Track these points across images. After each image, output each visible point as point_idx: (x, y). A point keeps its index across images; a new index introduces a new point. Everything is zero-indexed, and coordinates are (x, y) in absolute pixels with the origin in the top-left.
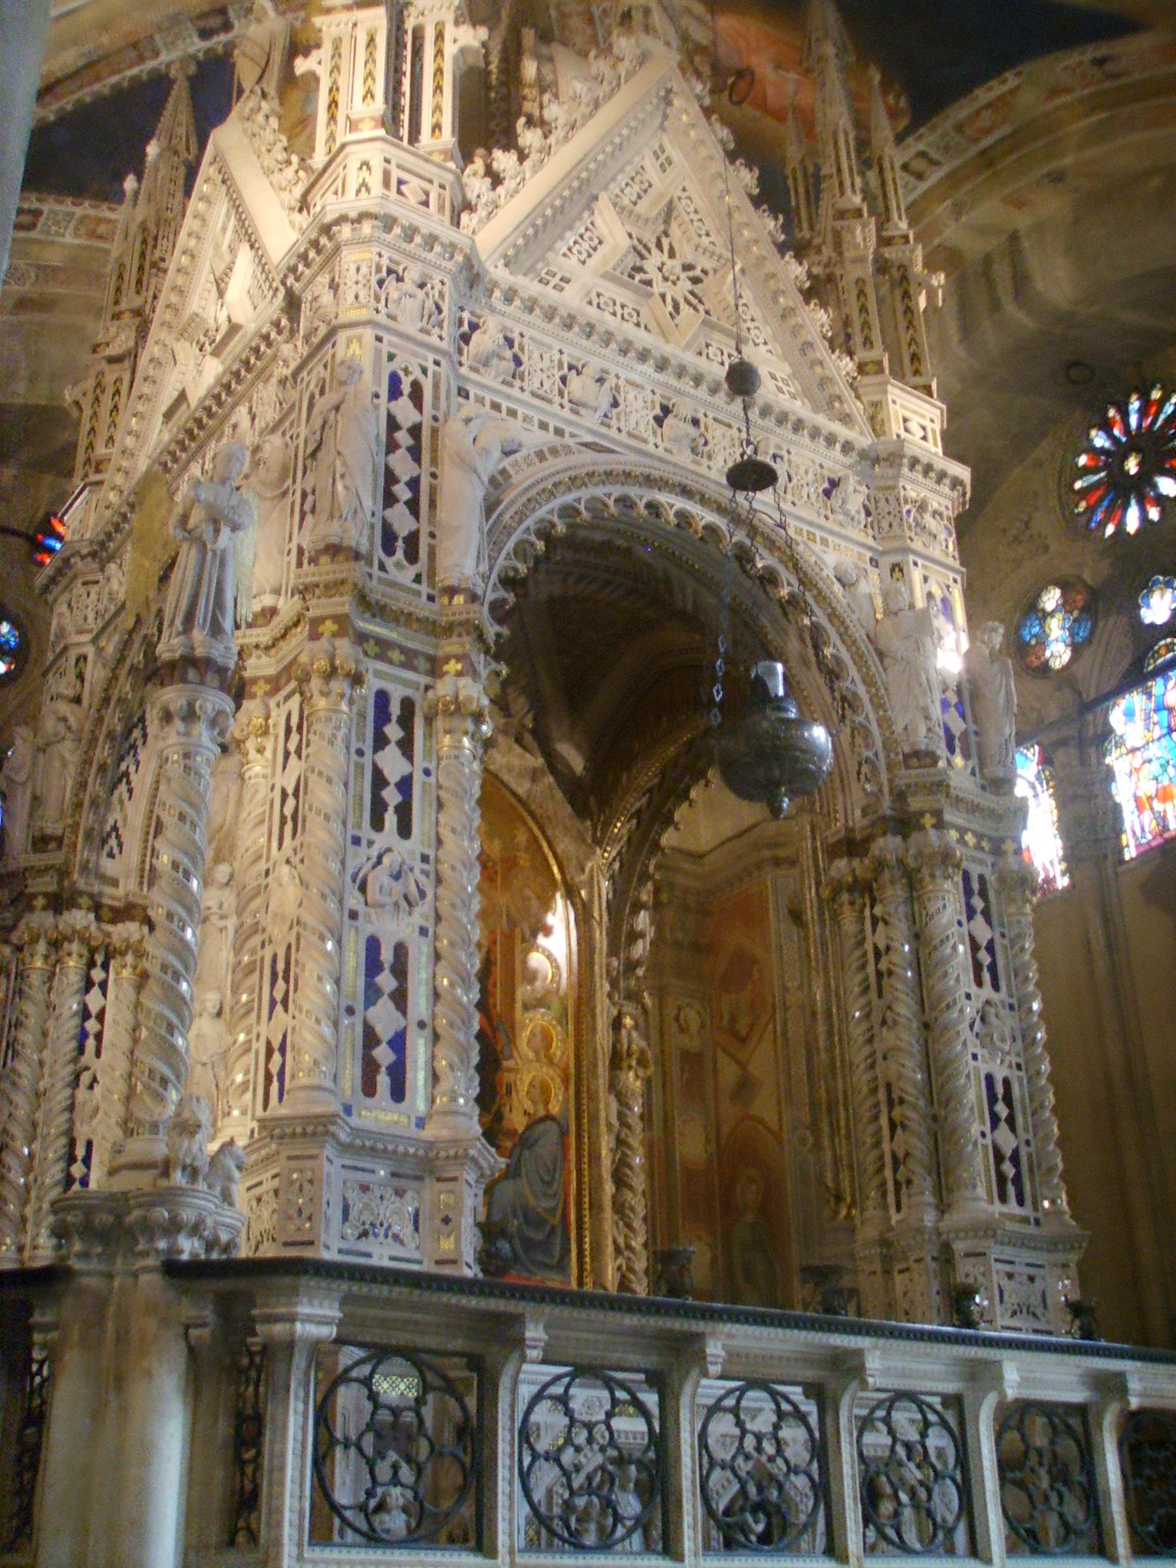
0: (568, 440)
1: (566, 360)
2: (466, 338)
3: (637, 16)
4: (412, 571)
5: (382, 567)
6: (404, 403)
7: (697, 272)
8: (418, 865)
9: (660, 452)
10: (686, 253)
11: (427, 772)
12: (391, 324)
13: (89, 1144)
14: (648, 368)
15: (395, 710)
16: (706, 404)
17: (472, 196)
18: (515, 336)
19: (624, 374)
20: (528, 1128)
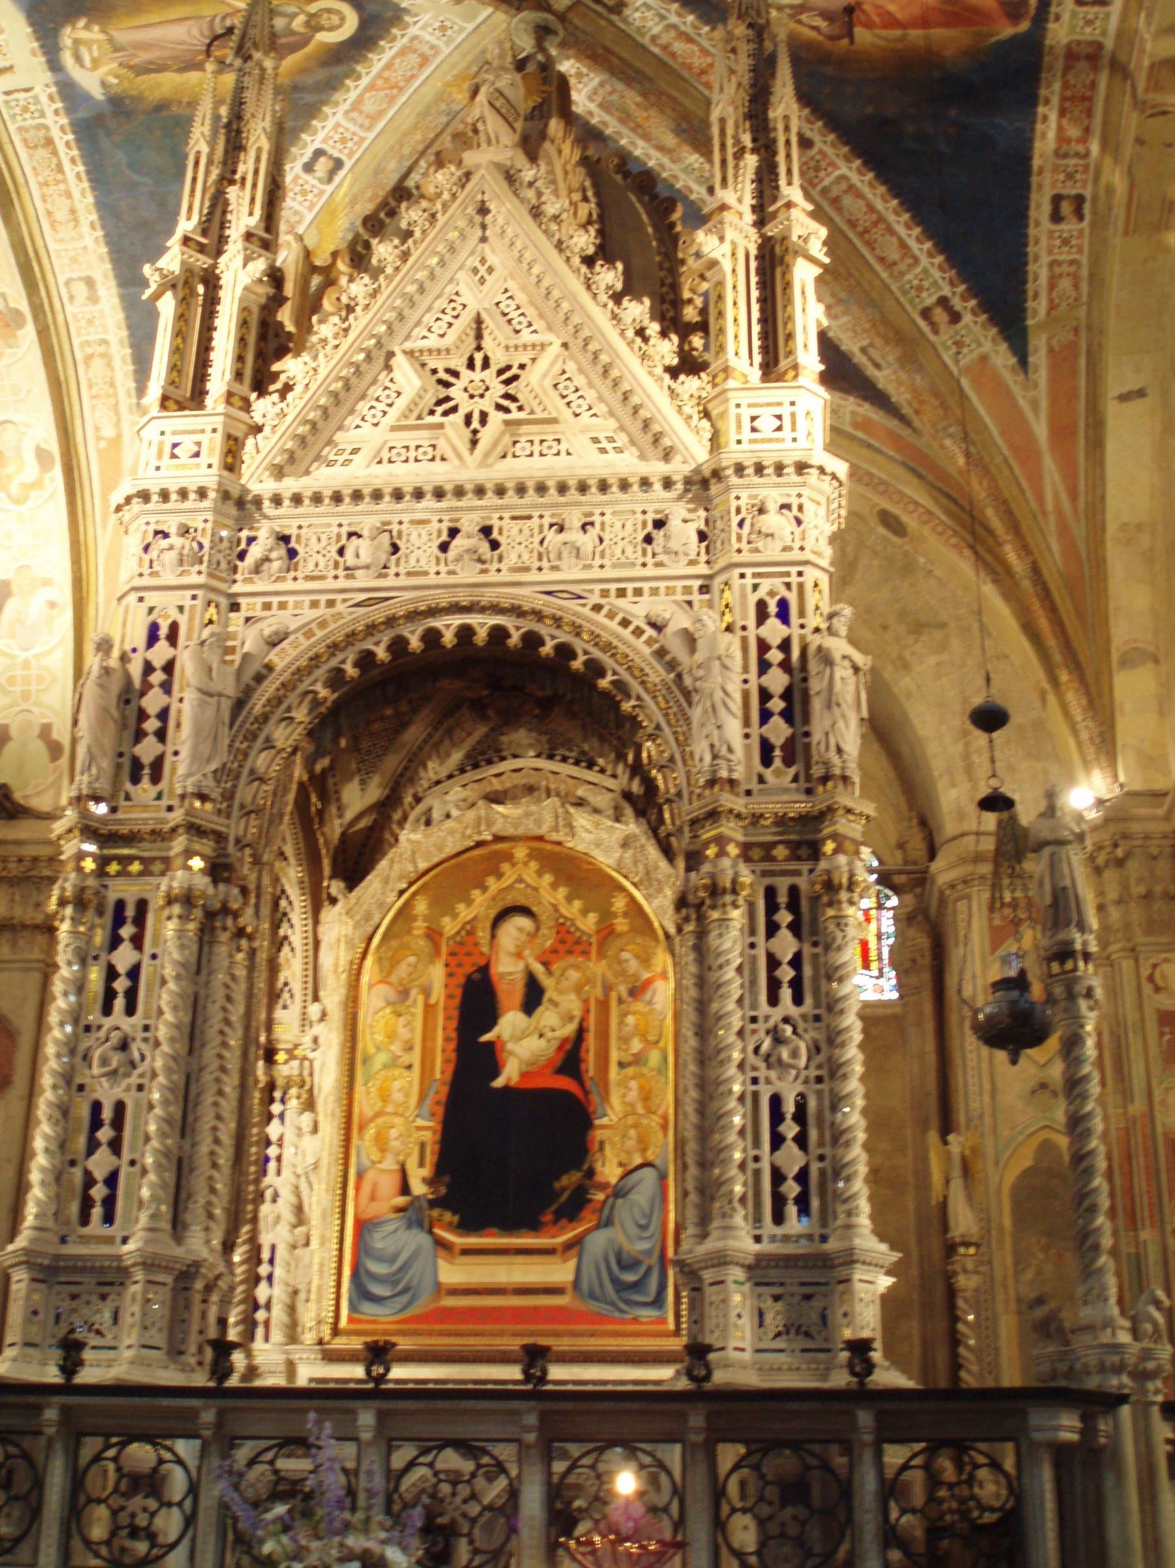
1: (344, 531)
2: (242, 556)
3: (480, 126)
4: (153, 791)
5: (128, 798)
7: (515, 371)
8: (140, 1035)
9: (444, 579)
10: (499, 358)
13: (273, 1248)
14: (429, 502)
15: (130, 912)
17: (258, 418)
18: (293, 532)
20: (623, 1178)
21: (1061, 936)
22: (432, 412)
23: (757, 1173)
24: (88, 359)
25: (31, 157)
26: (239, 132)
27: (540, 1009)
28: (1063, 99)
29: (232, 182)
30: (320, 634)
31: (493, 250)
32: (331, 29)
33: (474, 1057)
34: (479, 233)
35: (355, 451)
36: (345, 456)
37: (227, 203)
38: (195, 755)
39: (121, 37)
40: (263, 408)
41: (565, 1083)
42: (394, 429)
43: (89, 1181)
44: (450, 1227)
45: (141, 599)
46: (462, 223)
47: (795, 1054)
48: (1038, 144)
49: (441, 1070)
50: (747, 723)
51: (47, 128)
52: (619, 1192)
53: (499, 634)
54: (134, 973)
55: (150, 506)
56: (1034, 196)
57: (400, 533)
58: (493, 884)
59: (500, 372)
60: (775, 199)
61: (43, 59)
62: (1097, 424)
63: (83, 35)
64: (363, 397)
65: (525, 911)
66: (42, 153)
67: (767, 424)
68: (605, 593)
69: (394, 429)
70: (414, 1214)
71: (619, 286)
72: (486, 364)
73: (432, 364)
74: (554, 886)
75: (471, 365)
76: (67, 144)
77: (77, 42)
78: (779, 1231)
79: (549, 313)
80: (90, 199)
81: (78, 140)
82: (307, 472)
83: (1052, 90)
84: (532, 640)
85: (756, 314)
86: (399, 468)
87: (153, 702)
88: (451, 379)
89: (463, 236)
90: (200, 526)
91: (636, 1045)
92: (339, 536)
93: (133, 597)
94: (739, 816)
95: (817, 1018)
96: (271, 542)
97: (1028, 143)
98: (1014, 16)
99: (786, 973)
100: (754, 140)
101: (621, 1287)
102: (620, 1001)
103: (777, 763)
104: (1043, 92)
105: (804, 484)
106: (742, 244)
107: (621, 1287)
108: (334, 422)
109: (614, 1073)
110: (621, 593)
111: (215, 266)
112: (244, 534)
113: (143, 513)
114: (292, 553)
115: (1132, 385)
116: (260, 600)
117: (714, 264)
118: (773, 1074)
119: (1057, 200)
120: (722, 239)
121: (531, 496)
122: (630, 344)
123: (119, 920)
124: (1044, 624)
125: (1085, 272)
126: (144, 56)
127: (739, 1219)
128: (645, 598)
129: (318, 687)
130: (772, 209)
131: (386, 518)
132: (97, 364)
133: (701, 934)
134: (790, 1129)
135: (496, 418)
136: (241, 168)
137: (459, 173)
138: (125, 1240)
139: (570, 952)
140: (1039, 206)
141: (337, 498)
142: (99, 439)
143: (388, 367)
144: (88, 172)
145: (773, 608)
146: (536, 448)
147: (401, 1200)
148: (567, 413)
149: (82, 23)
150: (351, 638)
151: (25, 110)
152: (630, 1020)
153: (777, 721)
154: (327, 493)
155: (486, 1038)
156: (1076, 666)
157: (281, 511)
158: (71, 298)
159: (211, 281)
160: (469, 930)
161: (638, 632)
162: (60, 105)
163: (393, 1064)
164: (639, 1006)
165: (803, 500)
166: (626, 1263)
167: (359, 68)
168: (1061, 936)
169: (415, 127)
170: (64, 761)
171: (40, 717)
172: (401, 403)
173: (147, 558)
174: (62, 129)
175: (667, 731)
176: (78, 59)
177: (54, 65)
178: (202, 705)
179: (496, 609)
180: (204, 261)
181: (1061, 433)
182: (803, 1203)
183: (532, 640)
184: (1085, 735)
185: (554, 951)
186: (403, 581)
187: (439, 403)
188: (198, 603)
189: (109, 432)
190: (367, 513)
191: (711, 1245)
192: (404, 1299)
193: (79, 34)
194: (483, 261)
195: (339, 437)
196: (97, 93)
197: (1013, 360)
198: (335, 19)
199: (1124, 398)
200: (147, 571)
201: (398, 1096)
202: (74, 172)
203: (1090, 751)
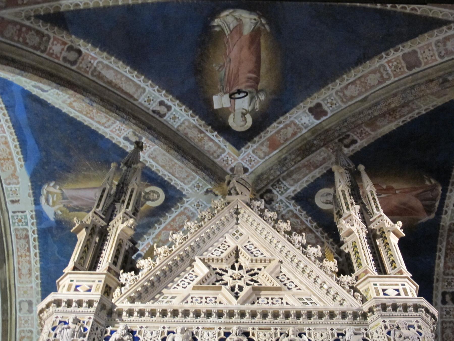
1: (166, 331)
7: (256, 271)
14: (214, 318)
16: (251, 324)
17: (122, 281)
18: (138, 329)
19: (201, 326)
25: (17, 242)
26: (123, 188)
28: (447, 249)
31: (242, 227)
32: (153, 200)
34: (235, 221)
35: (172, 298)
36: (168, 299)
37: (115, 208)
39: (68, 193)
42: (194, 288)
51: (27, 231)
55: (60, 309)
57: (197, 333)
61: (32, 199)
63: (52, 189)
64: (179, 276)
66: (23, 242)
67: (392, 293)
69: (194, 288)
72: (241, 268)
73: (213, 266)
76: (34, 240)
77: (48, 192)
80: (38, 265)
81: (39, 238)
85: (372, 258)
88: (223, 273)
90: (86, 320)
92: (163, 333)
96: (125, 331)
97: (432, 269)
98: (429, 212)
100: (355, 201)
104: (439, 246)
105: (419, 317)
106: (361, 231)
108: (163, 285)
111: (108, 225)
112: (109, 329)
113: (55, 312)
119: (444, 294)
120: (353, 225)
121: (269, 319)
126: (75, 203)
130: (371, 220)
131: (189, 325)
135: (246, 289)
136: (123, 198)
137: (224, 202)
140: (437, 296)
141: (164, 313)
143: (192, 266)
144: (40, 253)
148: (286, 288)
149: (52, 184)
151: (20, 221)
157: (132, 318)
158: (20, 309)
159: (103, 235)
162: (35, 221)
165: (420, 324)
167: (161, 219)
173: (53, 333)
174: (34, 232)
176: (47, 200)
177: (37, 202)
187: (218, 281)
190: (180, 323)
193: (50, 188)
194: (237, 231)
195: (164, 291)
196: (52, 217)
198: (156, 196)
202: (34, 251)
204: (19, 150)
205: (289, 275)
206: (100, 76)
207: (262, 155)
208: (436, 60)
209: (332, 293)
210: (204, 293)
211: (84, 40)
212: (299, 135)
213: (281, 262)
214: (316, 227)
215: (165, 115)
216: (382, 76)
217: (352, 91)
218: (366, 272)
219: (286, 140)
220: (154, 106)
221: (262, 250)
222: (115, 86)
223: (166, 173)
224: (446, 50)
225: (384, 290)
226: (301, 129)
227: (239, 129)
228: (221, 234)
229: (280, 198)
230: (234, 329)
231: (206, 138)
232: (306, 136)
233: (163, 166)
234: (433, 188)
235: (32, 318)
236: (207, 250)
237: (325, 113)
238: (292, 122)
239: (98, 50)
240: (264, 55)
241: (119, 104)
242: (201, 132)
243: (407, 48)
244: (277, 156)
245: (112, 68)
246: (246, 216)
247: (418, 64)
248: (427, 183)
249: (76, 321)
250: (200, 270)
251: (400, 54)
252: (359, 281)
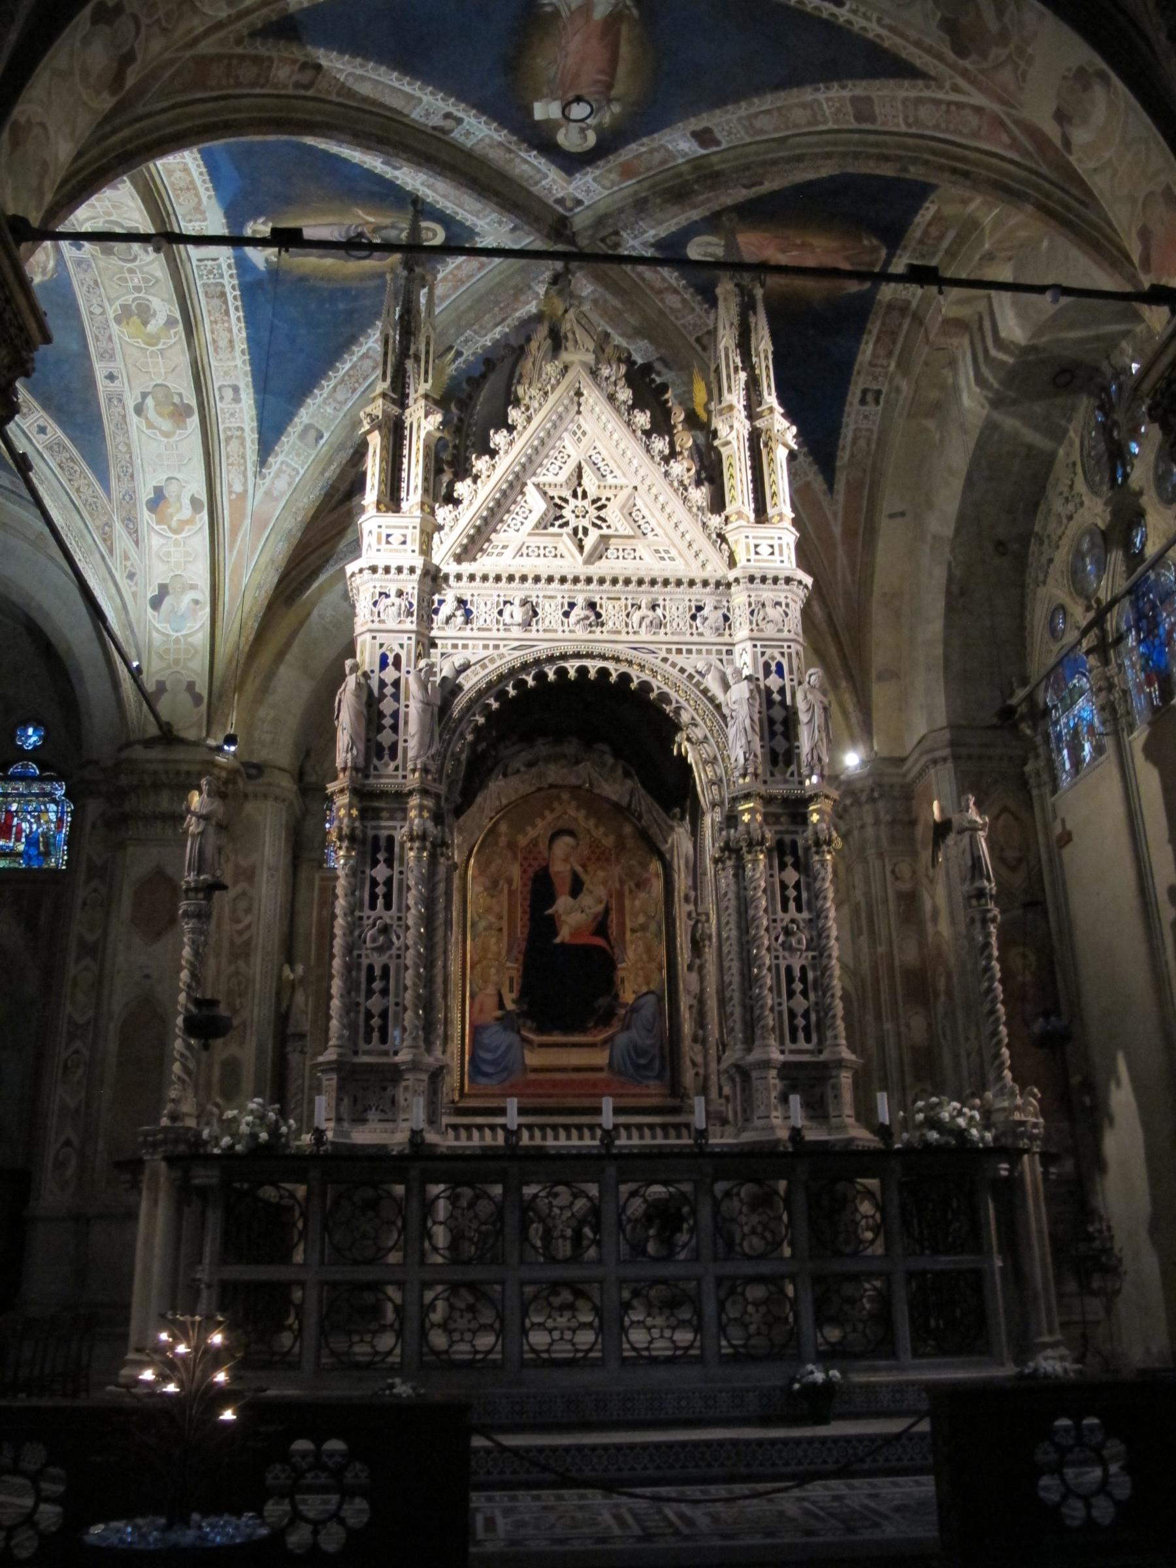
0: (502, 650)
1: (502, 600)
2: (436, 611)
3: (570, 335)
4: (392, 765)
5: (376, 768)
6: (390, 669)
7: (603, 501)
8: (395, 923)
9: (567, 635)
10: (592, 494)
11: (401, 873)
12: (382, 627)
14: (555, 585)
15: (383, 843)
17: (440, 521)
18: (468, 598)
21: (977, 884)
22: (552, 525)
23: (780, 1013)
24: (228, 439)
26: (409, 322)
27: (581, 896)
28: (880, 331)
29: (407, 356)
30: (491, 667)
33: (542, 925)
35: (504, 547)
38: (421, 744)
40: (443, 513)
41: (600, 941)
42: (530, 534)
43: (369, 1015)
44: (530, 1030)
45: (374, 638)
46: (566, 402)
47: (799, 942)
48: (860, 358)
49: (521, 932)
50: (762, 739)
52: (634, 1009)
53: (604, 673)
54: (388, 882)
55: (376, 576)
56: (852, 387)
58: (549, 817)
59: (594, 502)
60: (760, 404)
62: (871, 531)
64: (508, 511)
65: (571, 833)
66: (217, 302)
67: (764, 550)
68: (669, 651)
69: (530, 534)
70: (507, 1021)
71: (667, 452)
73: (551, 493)
74: (587, 818)
75: (575, 495)
76: (235, 298)
78: (793, 1047)
79: (624, 466)
80: (244, 334)
82: (475, 559)
83: (875, 326)
84: (625, 678)
86: (533, 560)
87: (387, 706)
89: (566, 408)
91: (641, 919)
93: (368, 636)
94: (762, 797)
95: (811, 920)
99: (792, 893)
101: (638, 1067)
102: (631, 891)
103: (781, 764)
104: (869, 326)
107: (638, 1067)
108: (490, 528)
109: (628, 935)
110: (679, 651)
112: (436, 597)
114: (468, 613)
115: (897, 509)
116: (450, 642)
117: (727, 443)
118: (787, 954)
119: (865, 392)
120: (731, 427)
121: (619, 586)
122: (676, 490)
123: (376, 848)
124: (833, 650)
125: (875, 437)
127: (772, 1041)
128: (694, 656)
129: (491, 701)
131: (528, 593)
132: (234, 444)
133: (740, 868)
134: (798, 986)
135: (594, 534)
138: (396, 1053)
139: (599, 859)
142: (230, 492)
143: (522, 493)
145: (773, 668)
146: (621, 554)
147: (499, 1013)
148: (639, 533)
149: (261, 220)
150: (513, 672)
151: (210, 272)
152: (637, 903)
153: (779, 738)
154: (492, 576)
155: (550, 911)
156: (850, 677)
158: (222, 398)
160: (534, 842)
161: (691, 677)
163: (489, 928)
164: (642, 895)
166: (640, 1051)
168: (977, 884)
169: (471, 308)
170: (204, 707)
171: (187, 676)
172: (534, 518)
173: (376, 610)
174: (233, 287)
175: (712, 740)
178: (424, 711)
179: (603, 657)
180: (396, 410)
181: (850, 533)
182: (807, 1030)
183: (625, 678)
184: (854, 720)
185: (589, 859)
186: (542, 635)
187: (557, 519)
188: (413, 642)
189: (238, 488)
191: (756, 1056)
192: (505, 1074)
194: (579, 427)
195: (493, 536)
196: (261, 266)
197: (825, 487)
198: (430, 234)
199: (892, 516)
200: (376, 619)
201: (494, 948)
202: (236, 317)
203: (857, 730)
204: (207, 178)
205: (645, 512)
206: (351, 94)
207: (608, 184)
208: (898, 125)
209: (695, 547)
210: (541, 541)
211: (326, 48)
212: (671, 164)
213: (635, 488)
214: (684, 287)
215: (452, 131)
216: (814, 115)
217: (762, 122)
218: (740, 514)
219: (648, 169)
220: (436, 121)
221: (613, 466)
222: (374, 102)
223: (449, 204)
224: (917, 121)
225: (756, 546)
226: (674, 158)
227: (573, 150)
228: (557, 434)
229: (631, 242)
230: (580, 601)
231: (518, 160)
232: (683, 168)
233: (443, 196)
234: (874, 250)
235: (241, 410)
236: (541, 465)
237: (718, 143)
238: (662, 146)
239: (347, 57)
240: (625, 50)
241: (380, 133)
242: (510, 151)
243: (860, 88)
244: (631, 190)
245: (370, 79)
246: (591, 401)
247: (872, 119)
248: (866, 242)
249: (400, 594)
250: (534, 504)
251: (846, 93)
252: (730, 527)
